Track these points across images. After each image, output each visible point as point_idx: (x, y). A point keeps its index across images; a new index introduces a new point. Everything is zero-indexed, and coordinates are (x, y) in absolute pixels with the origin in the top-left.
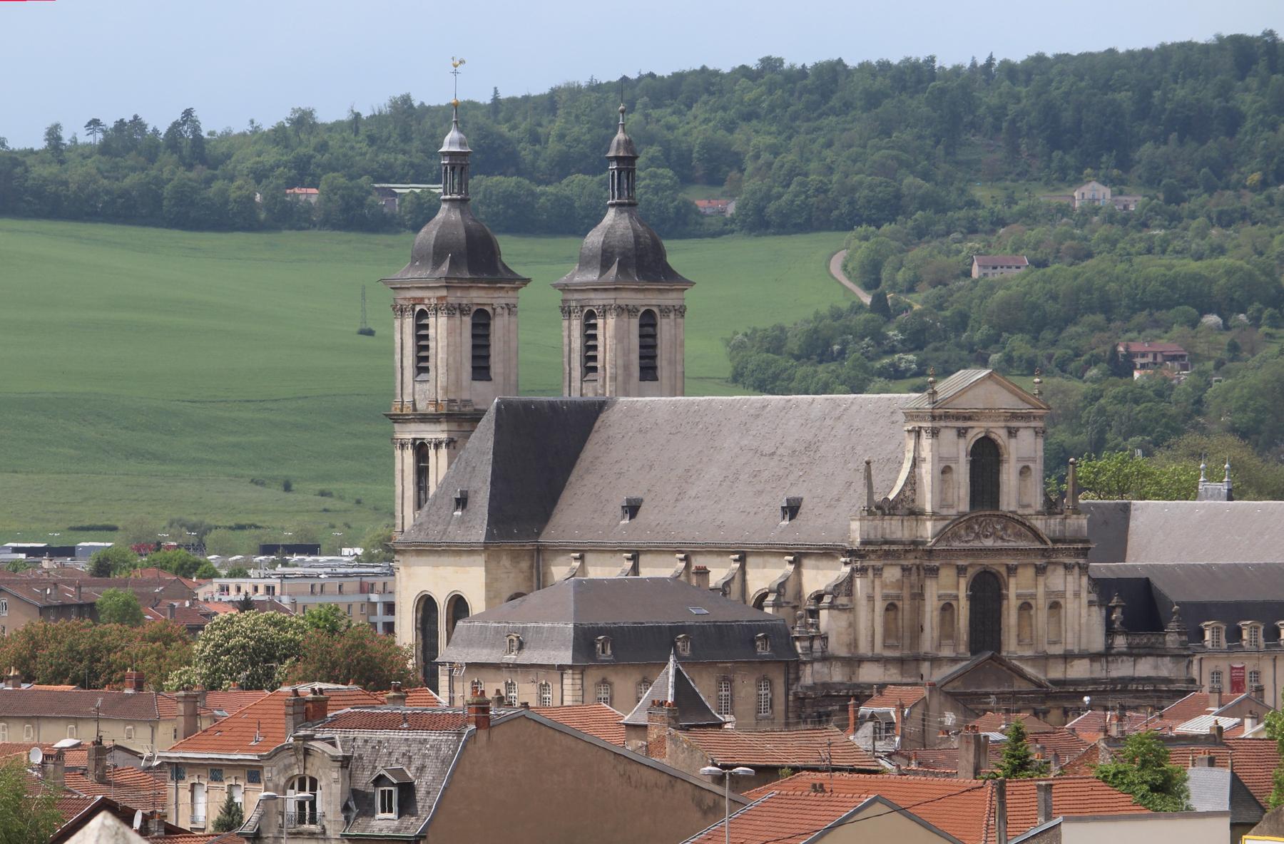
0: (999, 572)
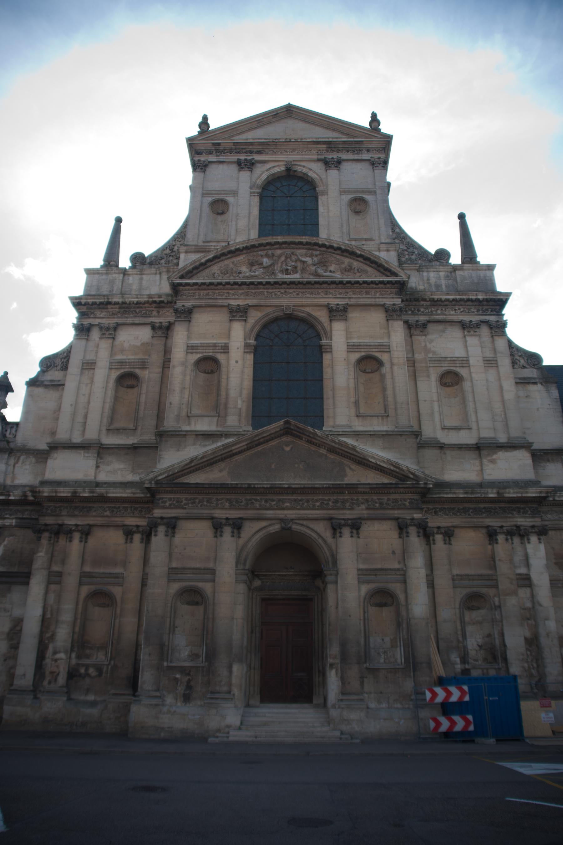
0: (316, 319)
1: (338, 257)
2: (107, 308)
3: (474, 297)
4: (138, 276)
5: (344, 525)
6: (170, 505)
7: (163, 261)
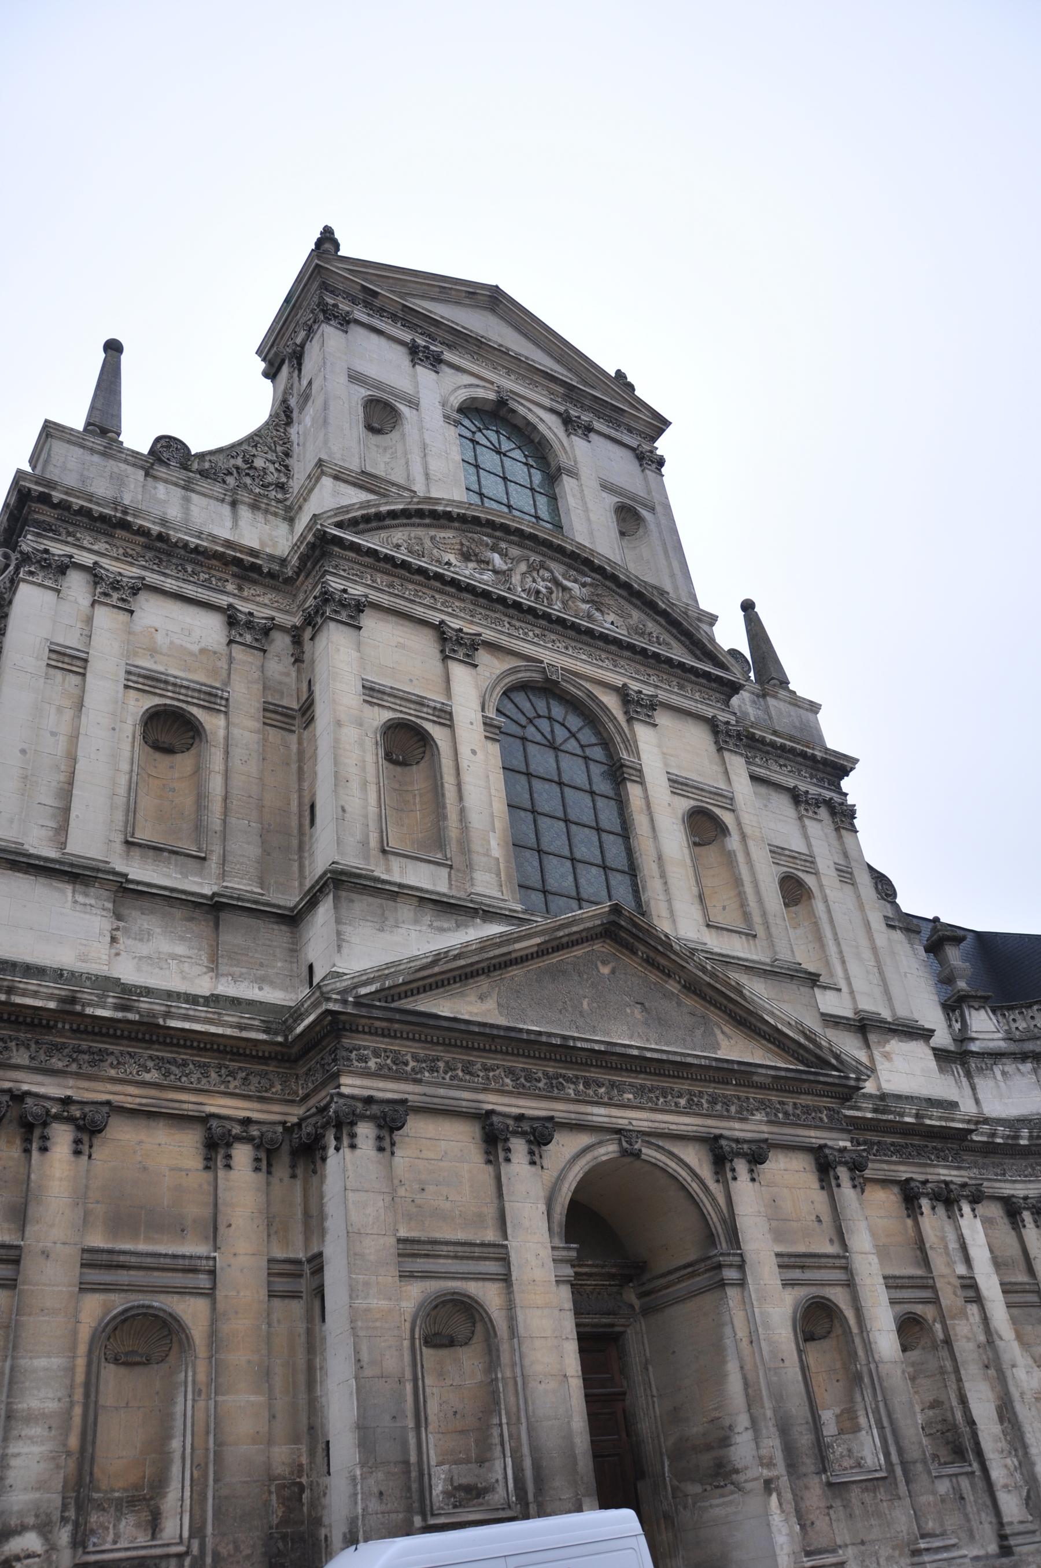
1: (621, 600)
2: (112, 536)
4: (179, 490)
5: (739, 1154)
6: (381, 1067)
7: (230, 480)
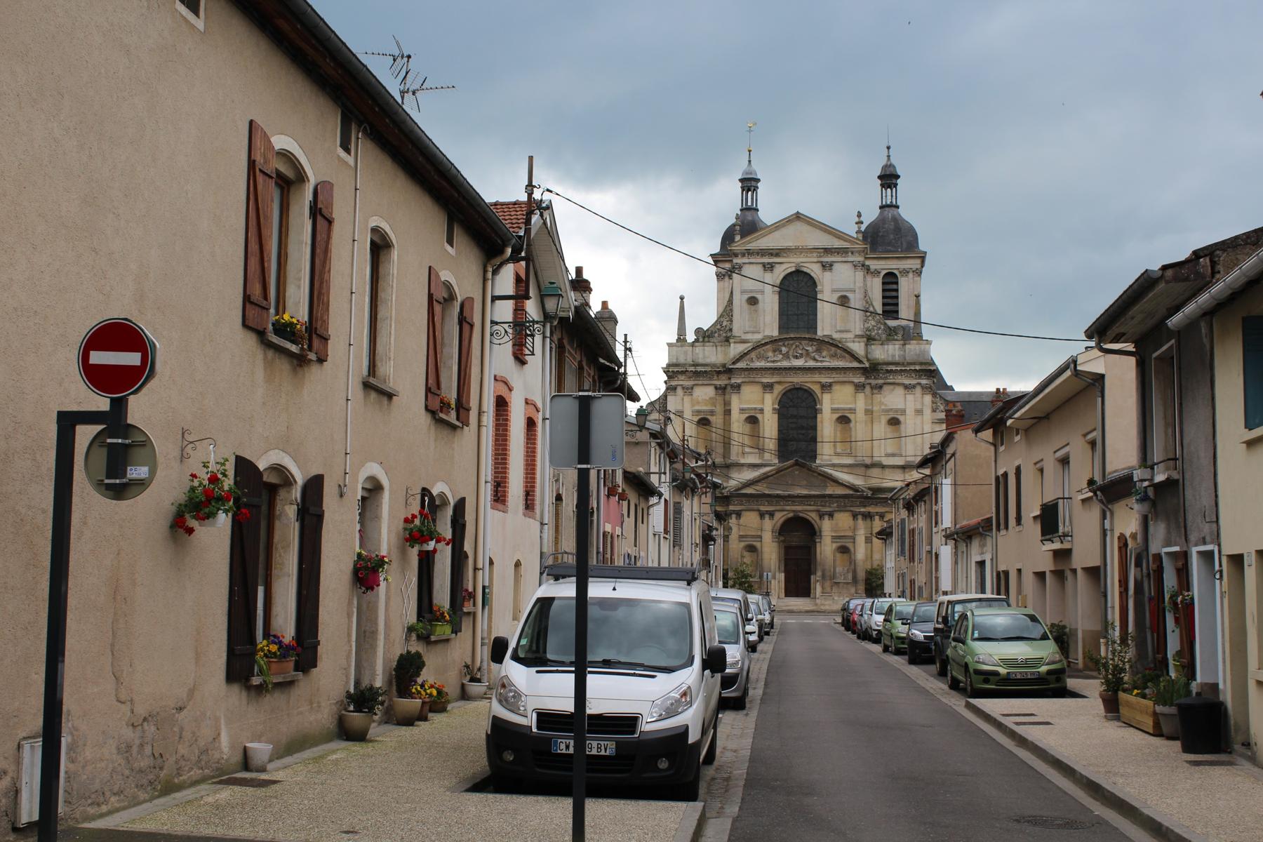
3: (913, 368)
7: (716, 335)
